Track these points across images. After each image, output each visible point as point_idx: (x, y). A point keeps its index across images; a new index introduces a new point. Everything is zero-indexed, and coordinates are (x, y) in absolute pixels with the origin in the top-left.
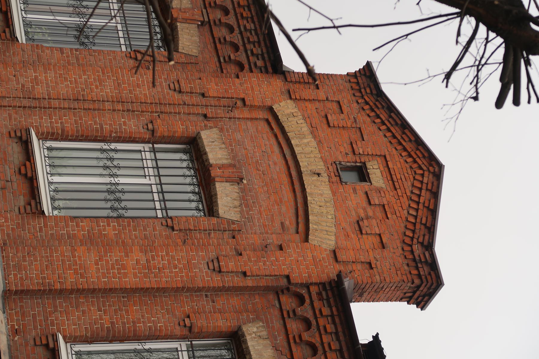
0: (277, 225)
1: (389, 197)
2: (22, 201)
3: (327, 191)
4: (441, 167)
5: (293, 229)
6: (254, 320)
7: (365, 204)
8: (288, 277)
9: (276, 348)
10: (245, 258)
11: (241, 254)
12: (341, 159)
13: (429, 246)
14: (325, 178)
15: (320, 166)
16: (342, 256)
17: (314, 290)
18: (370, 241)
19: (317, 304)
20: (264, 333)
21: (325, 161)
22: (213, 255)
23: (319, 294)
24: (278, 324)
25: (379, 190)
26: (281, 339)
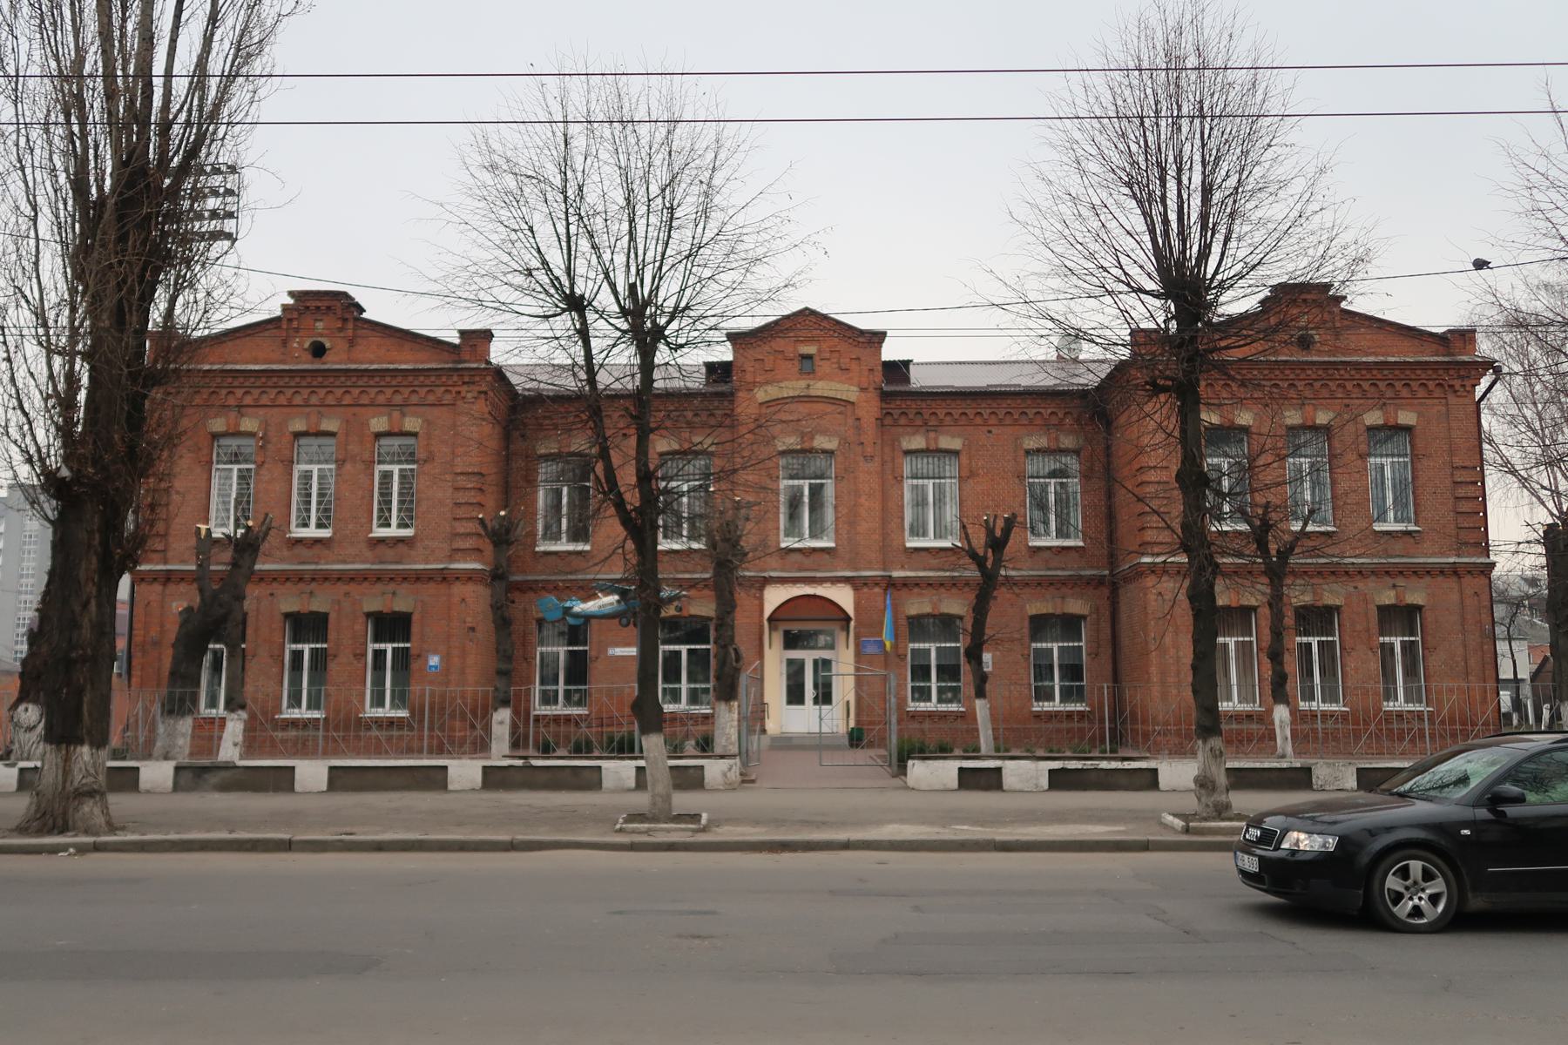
0: (839, 416)
1: (824, 346)
2: (827, 556)
3: (820, 384)
4: (807, 309)
5: (843, 408)
6: (900, 442)
7: (829, 362)
8: (877, 419)
9: (914, 434)
10: (864, 441)
11: (862, 443)
12: (797, 369)
13: (862, 332)
14: (812, 383)
15: (803, 384)
16: (865, 386)
17: (884, 406)
18: (854, 366)
19: (892, 406)
20: (907, 438)
21: (798, 379)
22: (862, 459)
23: (887, 403)
24: (901, 430)
25: (819, 351)
26: (909, 429)
